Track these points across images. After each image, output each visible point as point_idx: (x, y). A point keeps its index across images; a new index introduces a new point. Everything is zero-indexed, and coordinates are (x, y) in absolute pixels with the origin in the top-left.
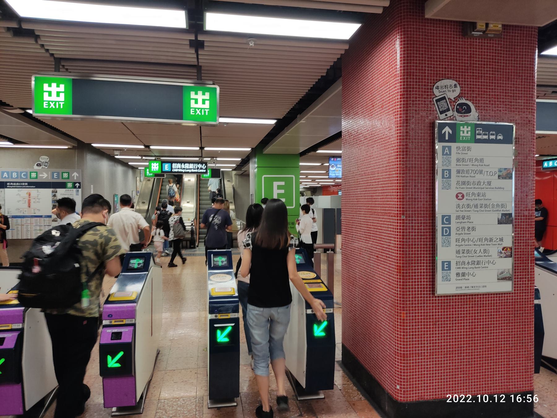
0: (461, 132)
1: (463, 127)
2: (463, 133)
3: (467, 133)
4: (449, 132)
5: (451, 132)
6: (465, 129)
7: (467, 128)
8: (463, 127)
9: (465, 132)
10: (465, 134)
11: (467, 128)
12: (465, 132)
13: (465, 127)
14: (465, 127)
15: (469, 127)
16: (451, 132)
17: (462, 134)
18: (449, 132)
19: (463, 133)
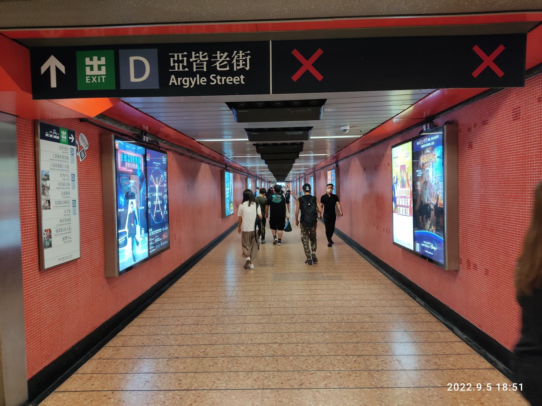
0: (88, 69)
1: (91, 60)
2: (92, 69)
3: (100, 69)
4: (57, 70)
5: (62, 69)
6: (95, 62)
7: (99, 59)
8: (91, 60)
9: (96, 68)
10: (96, 72)
11: (99, 59)
12: (96, 68)
13: (95, 58)
14: (95, 58)
15: (103, 59)
16: (62, 69)
17: (88, 72)
18: (57, 70)
19: (92, 69)
